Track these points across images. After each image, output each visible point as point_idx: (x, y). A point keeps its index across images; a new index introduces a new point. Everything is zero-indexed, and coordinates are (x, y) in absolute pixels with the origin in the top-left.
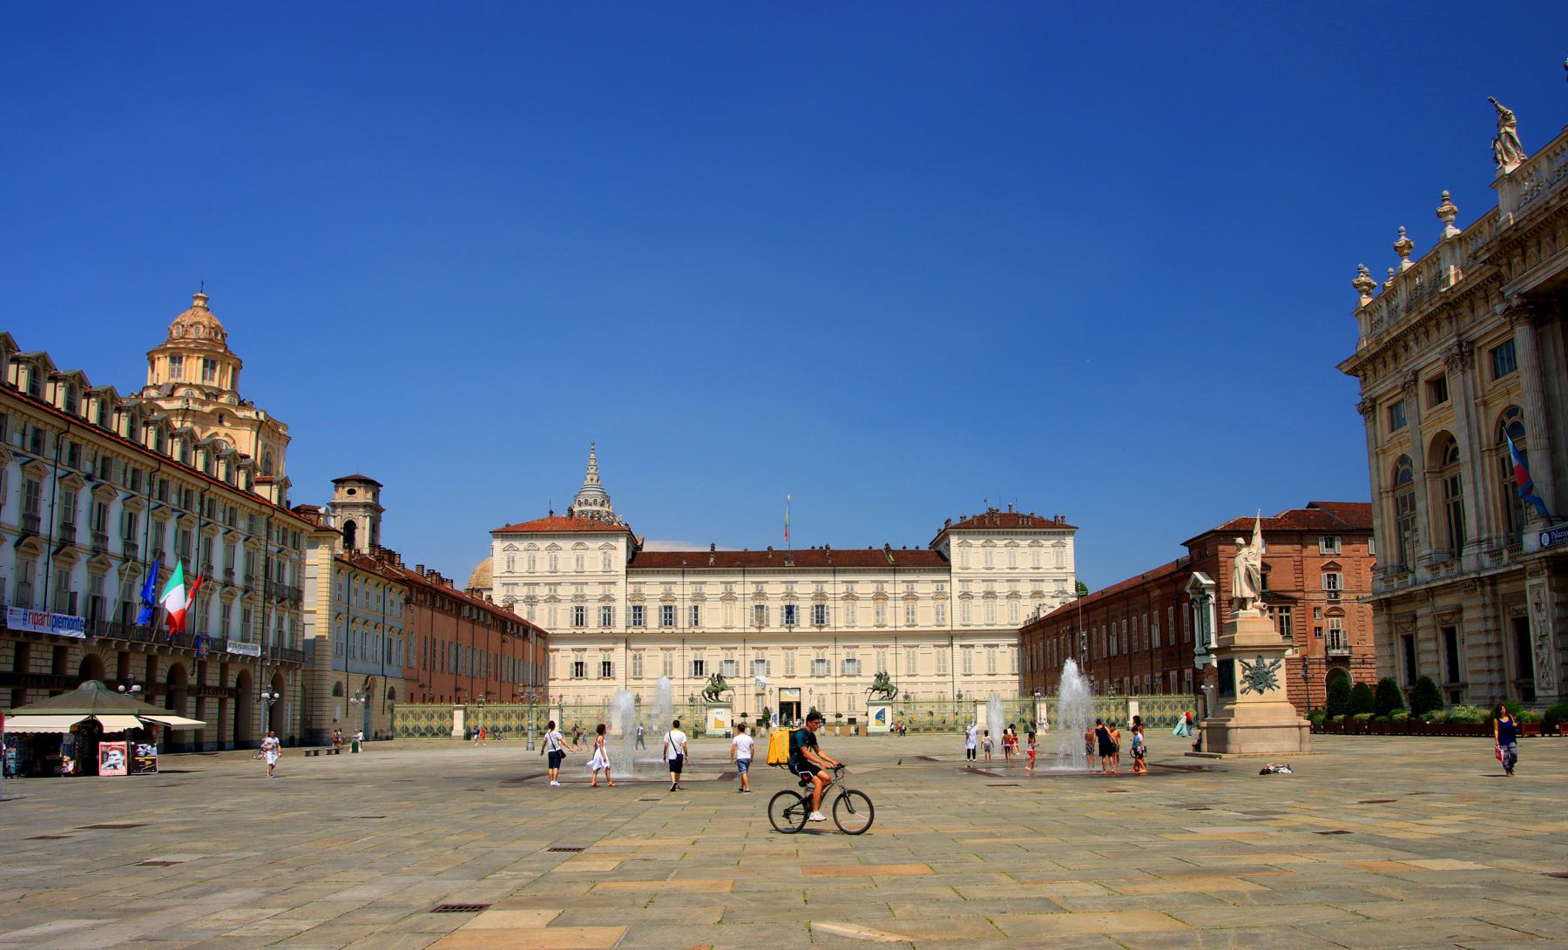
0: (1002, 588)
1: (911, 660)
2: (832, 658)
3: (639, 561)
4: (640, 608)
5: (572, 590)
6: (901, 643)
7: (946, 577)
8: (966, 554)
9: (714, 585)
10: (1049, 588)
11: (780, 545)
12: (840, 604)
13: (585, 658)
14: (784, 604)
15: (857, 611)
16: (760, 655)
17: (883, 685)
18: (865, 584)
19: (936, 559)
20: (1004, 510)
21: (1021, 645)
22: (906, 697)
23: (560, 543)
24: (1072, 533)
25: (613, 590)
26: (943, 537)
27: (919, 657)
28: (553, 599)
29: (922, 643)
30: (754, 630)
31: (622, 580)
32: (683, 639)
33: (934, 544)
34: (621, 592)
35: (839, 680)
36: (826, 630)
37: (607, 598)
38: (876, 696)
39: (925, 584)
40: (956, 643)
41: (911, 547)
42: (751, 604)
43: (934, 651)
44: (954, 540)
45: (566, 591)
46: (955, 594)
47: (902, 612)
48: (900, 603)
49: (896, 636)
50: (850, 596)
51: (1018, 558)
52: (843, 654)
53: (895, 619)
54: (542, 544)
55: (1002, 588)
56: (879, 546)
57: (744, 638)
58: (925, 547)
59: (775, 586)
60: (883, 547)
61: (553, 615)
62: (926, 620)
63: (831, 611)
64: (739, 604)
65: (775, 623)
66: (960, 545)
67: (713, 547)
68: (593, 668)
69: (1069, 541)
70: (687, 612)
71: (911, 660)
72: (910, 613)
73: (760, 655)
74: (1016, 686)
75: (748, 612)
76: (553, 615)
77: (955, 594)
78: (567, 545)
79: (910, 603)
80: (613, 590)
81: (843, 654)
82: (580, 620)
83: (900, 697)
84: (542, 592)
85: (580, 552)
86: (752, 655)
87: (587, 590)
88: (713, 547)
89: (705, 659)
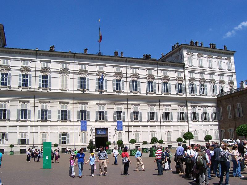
4: (6, 74)
6: (162, 104)
8: (191, 60)
9: (55, 65)
14: (96, 77)
21: (217, 107)
24: (232, 54)
26: (178, 49)
29: (172, 104)
32: (35, 95)
36: (122, 94)
40: (189, 104)
44: (185, 52)
46: (187, 79)
57: (73, 97)
63: (125, 83)
64: (71, 76)
69: (232, 58)
70: (38, 79)
74: (217, 128)
75: (76, 81)
77: (187, 79)
89: (48, 109)
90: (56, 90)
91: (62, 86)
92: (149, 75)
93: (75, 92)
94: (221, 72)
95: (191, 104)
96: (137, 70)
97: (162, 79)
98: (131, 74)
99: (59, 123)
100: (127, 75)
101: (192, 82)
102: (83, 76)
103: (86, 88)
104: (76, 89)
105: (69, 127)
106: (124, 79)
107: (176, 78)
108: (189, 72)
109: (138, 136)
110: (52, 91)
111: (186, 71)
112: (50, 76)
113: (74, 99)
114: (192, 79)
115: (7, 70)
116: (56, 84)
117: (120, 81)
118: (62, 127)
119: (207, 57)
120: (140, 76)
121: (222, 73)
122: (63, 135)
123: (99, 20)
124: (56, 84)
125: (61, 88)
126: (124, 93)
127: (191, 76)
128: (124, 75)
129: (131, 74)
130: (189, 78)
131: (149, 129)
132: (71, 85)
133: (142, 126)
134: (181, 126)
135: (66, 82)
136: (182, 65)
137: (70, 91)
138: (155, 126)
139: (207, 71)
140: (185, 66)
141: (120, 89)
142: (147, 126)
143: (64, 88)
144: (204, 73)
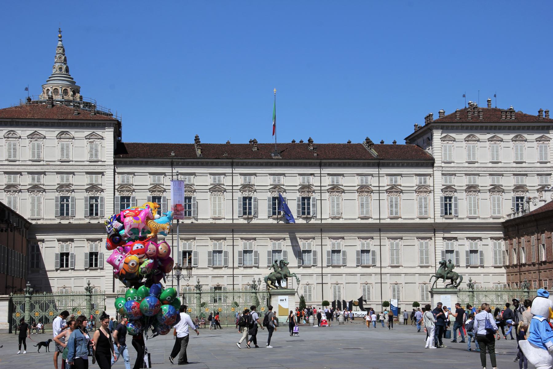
0: (485, 182)
1: (395, 252)
2: (318, 249)
3: (124, 153)
5: (56, 180)
6: (384, 235)
7: (428, 171)
9: (202, 178)
10: (533, 182)
11: (265, 138)
12: (326, 196)
13: (71, 248)
14: (270, 195)
15: (343, 204)
16: (248, 245)
17: (446, 271)
18: (351, 178)
19: (413, 152)
20: (483, 105)
22: (470, 285)
23: (42, 131)
25: (99, 180)
27: (401, 248)
28: (35, 188)
30: (242, 221)
31: (109, 172)
33: (410, 139)
34: (107, 182)
35: (325, 271)
36: (313, 221)
37: (93, 187)
38: (441, 284)
39: (409, 178)
41: (388, 142)
42: (239, 195)
43: (417, 242)
44: (437, 135)
45: (51, 181)
47: (385, 204)
48: (384, 196)
49: (380, 228)
50: (335, 189)
51: (501, 152)
52: (329, 245)
53: (380, 211)
54: (24, 132)
55: (485, 182)
56: (358, 139)
57: (232, 229)
58: (401, 142)
59: (263, 178)
60: (361, 140)
61: (36, 206)
62: (409, 212)
64: (228, 195)
65: (263, 215)
66: (443, 139)
67: (197, 139)
68: (80, 261)
71: (395, 252)
72: (393, 205)
73: (248, 245)
75: (236, 203)
76: (36, 206)
78: (51, 133)
79: (394, 196)
80: (99, 180)
81: (329, 245)
82: (64, 208)
83: (464, 286)
84: (26, 181)
85: (65, 142)
86: (241, 245)
87: (72, 180)
88: (197, 139)
89: (194, 249)
90: (203, 219)
91: (215, 212)
92: (362, 186)
93: (235, 222)
94: (521, 169)
95: (442, 235)
96: (340, 178)
97: (387, 191)
98: (329, 185)
99: (210, 271)
100: (323, 188)
101: (448, 194)
102: (246, 194)
103: (253, 214)
104: (236, 216)
105: (225, 276)
106: (316, 196)
107: (414, 188)
108: (443, 174)
109: (339, 292)
110: (200, 222)
111: (438, 174)
112: (194, 198)
113: (233, 231)
114: (448, 188)
115: (128, 191)
116: (207, 210)
117: (309, 199)
119: (490, 140)
120: (345, 188)
121: (524, 169)
122: (216, 288)
123: (275, 90)
124: (207, 210)
125: (213, 216)
126: (316, 219)
127: (446, 181)
128: (314, 188)
129: (329, 185)
130: (443, 185)
131: (358, 279)
132: (227, 210)
133: (347, 274)
134: (420, 274)
136: (430, 162)
137: (227, 219)
138: (370, 274)
139: (485, 169)
140: (435, 165)
141: (309, 213)
142: (355, 274)
143: (217, 216)
144: (478, 175)
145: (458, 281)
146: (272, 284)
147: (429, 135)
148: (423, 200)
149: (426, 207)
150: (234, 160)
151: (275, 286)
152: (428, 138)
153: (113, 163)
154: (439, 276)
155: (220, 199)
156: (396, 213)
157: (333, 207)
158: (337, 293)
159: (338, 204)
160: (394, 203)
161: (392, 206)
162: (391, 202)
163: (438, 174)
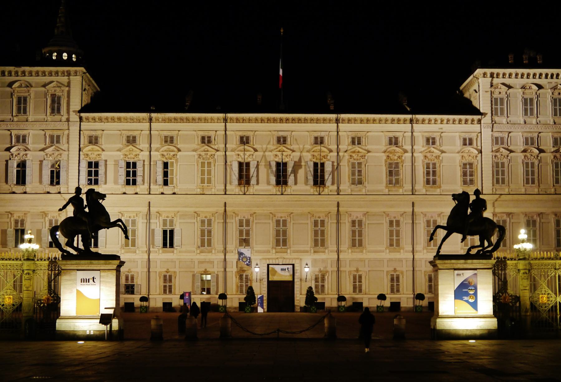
31: (74, 129)
38: (455, 244)
91: (203, 181)
118: (201, 262)
135: (209, 173)
138: (400, 260)
140: (482, 122)
145: (494, 239)
146: (68, 244)
147: (476, 87)
148: (468, 166)
149: (471, 175)
150: (229, 115)
151: (76, 249)
152: (475, 91)
153: (78, 120)
154: (450, 229)
155: (209, 164)
156: (434, 182)
157: (353, 174)
158: (357, 283)
159: (360, 171)
160: (431, 170)
161: (428, 173)
162: (428, 167)
163: (487, 134)
